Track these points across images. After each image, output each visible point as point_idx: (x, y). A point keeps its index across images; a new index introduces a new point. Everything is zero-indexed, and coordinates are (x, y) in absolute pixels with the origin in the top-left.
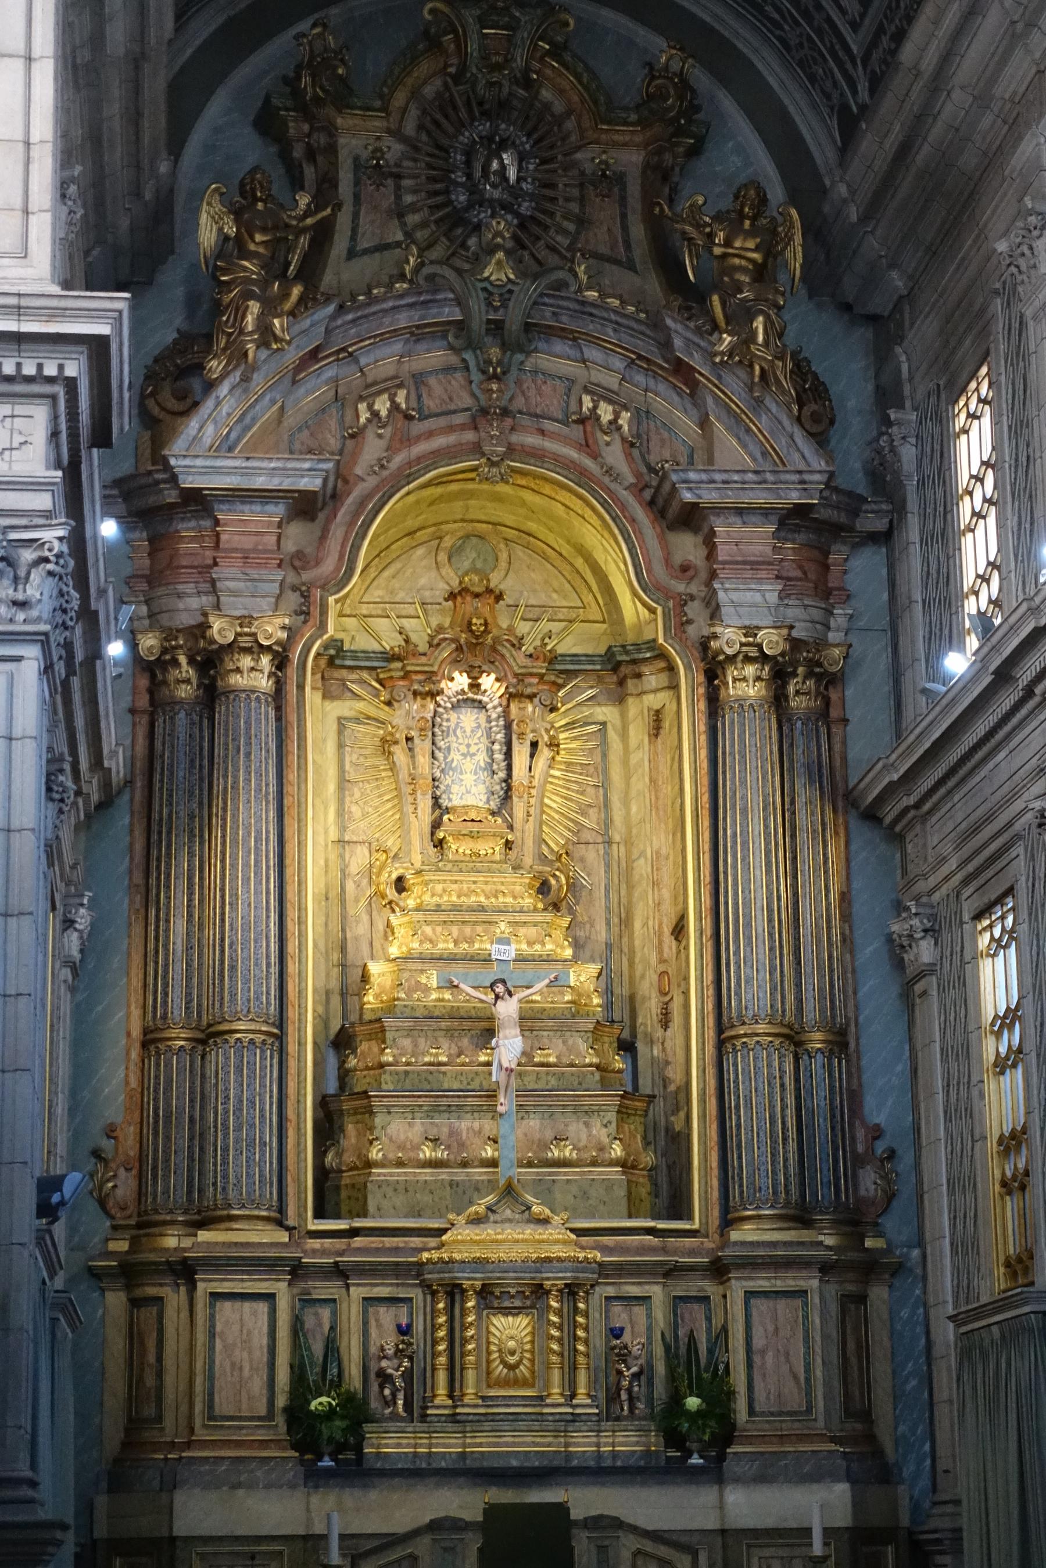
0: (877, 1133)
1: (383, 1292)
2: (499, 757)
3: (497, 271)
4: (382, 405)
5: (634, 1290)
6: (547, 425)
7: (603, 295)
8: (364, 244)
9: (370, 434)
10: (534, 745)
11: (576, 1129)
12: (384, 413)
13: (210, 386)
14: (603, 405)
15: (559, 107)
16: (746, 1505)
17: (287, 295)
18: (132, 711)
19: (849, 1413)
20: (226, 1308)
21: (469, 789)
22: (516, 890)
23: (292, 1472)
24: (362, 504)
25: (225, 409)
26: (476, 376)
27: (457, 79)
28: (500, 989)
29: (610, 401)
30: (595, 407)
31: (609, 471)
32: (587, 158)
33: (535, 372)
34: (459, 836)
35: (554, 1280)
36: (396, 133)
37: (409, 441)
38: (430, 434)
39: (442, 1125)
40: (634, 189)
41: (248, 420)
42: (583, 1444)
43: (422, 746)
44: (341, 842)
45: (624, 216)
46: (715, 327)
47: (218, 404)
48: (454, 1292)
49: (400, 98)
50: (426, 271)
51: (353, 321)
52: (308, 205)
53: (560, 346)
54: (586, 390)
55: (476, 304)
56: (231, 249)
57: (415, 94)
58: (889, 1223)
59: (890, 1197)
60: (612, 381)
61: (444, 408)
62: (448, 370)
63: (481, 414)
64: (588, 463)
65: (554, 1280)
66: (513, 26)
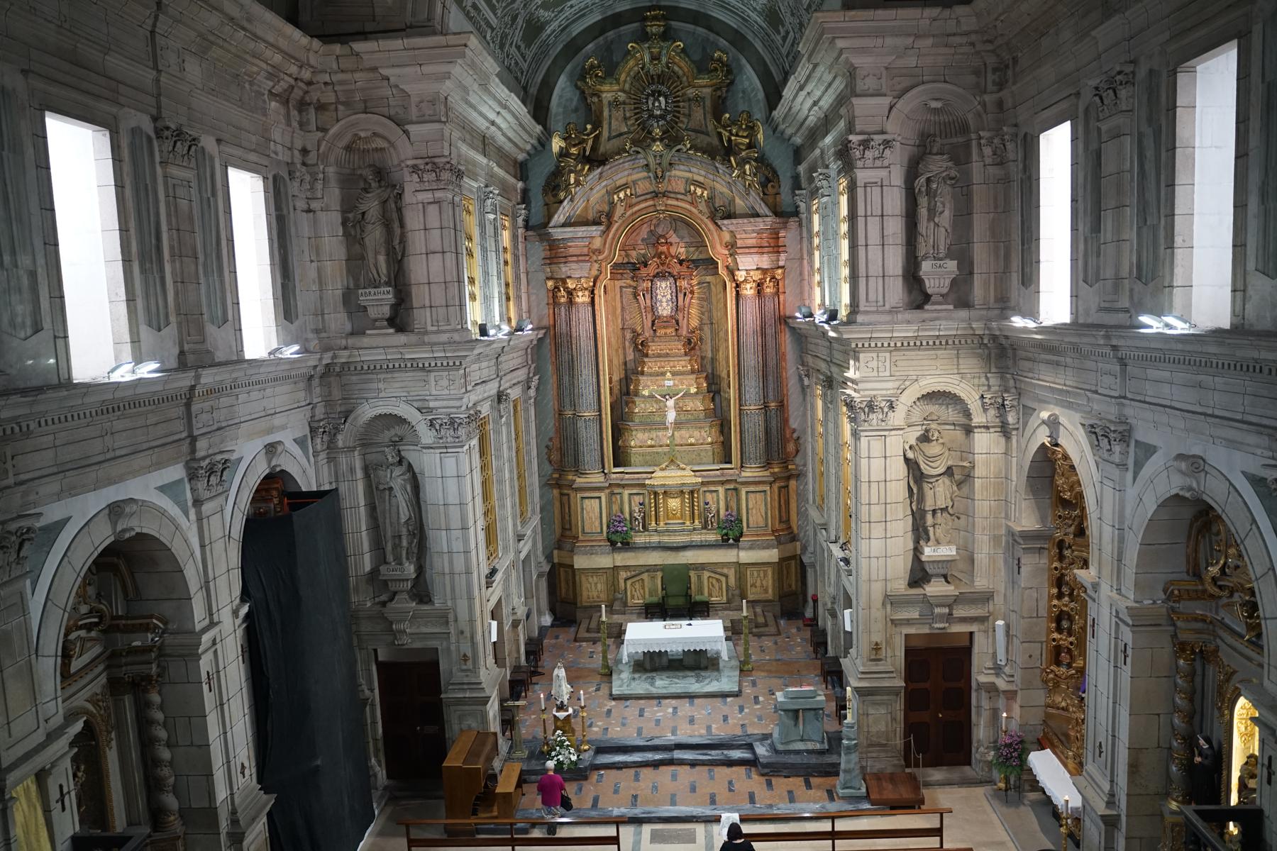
0: (794, 431)
1: (634, 491)
3: (658, 147)
4: (622, 195)
5: (713, 489)
11: (696, 433)
13: (561, 202)
15: (681, 73)
16: (745, 556)
19: (780, 522)
20: (586, 501)
21: (665, 309)
22: (678, 347)
23: (609, 548)
31: (701, 212)
32: (691, 92)
35: (686, 489)
36: (623, 91)
37: (631, 206)
38: (639, 203)
39: (654, 434)
40: (708, 103)
42: (697, 538)
43: (648, 296)
48: (656, 494)
49: (623, 76)
55: (651, 159)
56: (564, 154)
57: (628, 75)
58: (798, 460)
59: (797, 451)
60: (701, 179)
63: (656, 195)
65: (686, 489)
66: (661, 48)
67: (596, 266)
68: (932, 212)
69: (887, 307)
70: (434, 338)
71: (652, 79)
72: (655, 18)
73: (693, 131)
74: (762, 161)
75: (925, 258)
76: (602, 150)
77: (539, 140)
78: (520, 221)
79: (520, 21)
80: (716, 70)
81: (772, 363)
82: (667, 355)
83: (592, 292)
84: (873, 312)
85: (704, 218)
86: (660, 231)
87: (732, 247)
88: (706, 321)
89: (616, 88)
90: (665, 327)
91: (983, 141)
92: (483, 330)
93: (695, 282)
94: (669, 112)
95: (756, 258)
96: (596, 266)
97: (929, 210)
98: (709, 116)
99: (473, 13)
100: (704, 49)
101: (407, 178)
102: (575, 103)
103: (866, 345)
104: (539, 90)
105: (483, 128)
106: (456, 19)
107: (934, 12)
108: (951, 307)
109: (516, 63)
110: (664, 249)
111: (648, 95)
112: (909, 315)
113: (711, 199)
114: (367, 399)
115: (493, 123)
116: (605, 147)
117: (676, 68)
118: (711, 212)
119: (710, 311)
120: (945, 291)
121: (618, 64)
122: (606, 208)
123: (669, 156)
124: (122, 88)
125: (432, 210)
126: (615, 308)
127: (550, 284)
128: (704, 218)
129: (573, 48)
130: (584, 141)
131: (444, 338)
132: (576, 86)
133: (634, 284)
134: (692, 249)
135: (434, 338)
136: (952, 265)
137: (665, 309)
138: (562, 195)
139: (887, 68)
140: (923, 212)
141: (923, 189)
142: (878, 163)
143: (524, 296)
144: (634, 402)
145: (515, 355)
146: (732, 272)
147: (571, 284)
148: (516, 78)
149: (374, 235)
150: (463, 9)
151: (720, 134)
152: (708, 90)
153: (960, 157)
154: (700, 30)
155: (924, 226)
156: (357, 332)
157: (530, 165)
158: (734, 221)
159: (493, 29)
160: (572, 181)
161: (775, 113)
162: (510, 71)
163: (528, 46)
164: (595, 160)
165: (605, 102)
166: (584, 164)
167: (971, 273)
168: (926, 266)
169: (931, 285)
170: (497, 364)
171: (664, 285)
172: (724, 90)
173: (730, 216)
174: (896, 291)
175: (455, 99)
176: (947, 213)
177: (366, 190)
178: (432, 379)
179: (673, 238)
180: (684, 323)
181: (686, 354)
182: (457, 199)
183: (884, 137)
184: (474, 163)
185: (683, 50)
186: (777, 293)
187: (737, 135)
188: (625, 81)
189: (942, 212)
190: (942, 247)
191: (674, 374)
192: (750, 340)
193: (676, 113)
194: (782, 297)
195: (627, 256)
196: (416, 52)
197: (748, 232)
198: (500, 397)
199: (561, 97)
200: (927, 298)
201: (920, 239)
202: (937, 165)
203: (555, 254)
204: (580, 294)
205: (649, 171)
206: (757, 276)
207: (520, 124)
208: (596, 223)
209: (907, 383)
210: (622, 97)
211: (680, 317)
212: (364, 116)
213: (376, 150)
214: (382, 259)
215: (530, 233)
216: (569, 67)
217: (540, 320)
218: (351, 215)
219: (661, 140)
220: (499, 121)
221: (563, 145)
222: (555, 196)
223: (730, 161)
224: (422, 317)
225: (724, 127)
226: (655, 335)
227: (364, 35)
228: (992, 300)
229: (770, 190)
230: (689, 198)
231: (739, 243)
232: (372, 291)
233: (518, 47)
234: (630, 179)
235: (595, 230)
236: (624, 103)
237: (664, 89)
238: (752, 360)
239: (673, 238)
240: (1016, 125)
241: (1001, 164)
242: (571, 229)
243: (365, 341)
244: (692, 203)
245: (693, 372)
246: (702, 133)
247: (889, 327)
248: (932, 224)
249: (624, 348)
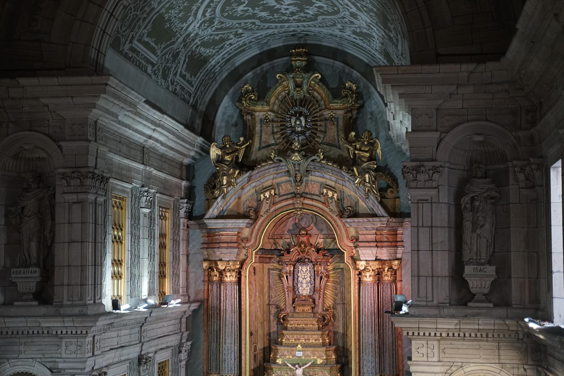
2: (313, 280)
3: (296, 157)
4: (267, 194)
6: (314, 197)
8: (263, 145)
9: (264, 203)
10: (321, 278)
12: (268, 197)
14: (329, 192)
15: (319, 97)
17: (235, 173)
18: (203, 281)
21: (305, 289)
22: (313, 323)
24: (262, 223)
25: (220, 204)
26: (294, 185)
27: (288, 94)
28: (297, 366)
29: (331, 190)
30: (327, 192)
33: (311, 181)
34: (299, 305)
36: (271, 111)
37: (274, 204)
38: (281, 201)
40: (341, 123)
41: (228, 204)
44: (269, 305)
45: (338, 131)
46: (355, 175)
47: (218, 204)
49: (273, 100)
50: (276, 158)
51: (258, 173)
52: (243, 141)
53: (317, 174)
54: (325, 188)
55: (291, 167)
56: (220, 160)
57: (277, 98)
60: (332, 184)
61: (286, 193)
62: (287, 181)
63: (295, 195)
64: (325, 209)
67: (244, 251)
68: (475, 225)
69: (435, 302)
70: (68, 311)
71: (295, 103)
72: (299, 54)
73: (328, 144)
74: (382, 170)
75: (469, 263)
76: (253, 157)
77: (202, 149)
78: (182, 212)
79: (182, 57)
80: (346, 96)
81: (388, 340)
82: (303, 329)
83: (240, 273)
84: (423, 306)
85: (334, 216)
86: (303, 224)
87: (355, 240)
88: (339, 301)
89: (267, 108)
90: (303, 305)
91: (516, 169)
92: (116, 305)
93: (330, 268)
94: (308, 129)
95: (374, 250)
96: (244, 251)
97: (473, 223)
98: (342, 135)
99: (130, 54)
100: (341, 79)
101: (58, 182)
102: (235, 119)
103: (416, 334)
104: (207, 108)
105: (142, 141)
106: (111, 60)
107: (471, 67)
108: (491, 305)
109: (183, 88)
110: (305, 239)
111: (292, 115)
112: (452, 311)
113: (340, 200)
114: (8, 359)
115: (150, 137)
116: (256, 154)
117: (316, 94)
118: (341, 211)
119: (343, 293)
120: (486, 291)
121: (270, 88)
122: (255, 204)
123: (305, 164)
125: (76, 208)
126: (262, 287)
127: (205, 265)
128: (334, 216)
129: (236, 75)
130: (237, 150)
131: (76, 310)
132: (235, 105)
133: (280, 267)
134: (329, 240)
135: (68, 311)
136: (491, 270)
137: (305, 289)
138: (217, 192)
139: (437, 109)
140: (467, 225)
141: (468, 206)
142: (428, 184)
143: (182, 275)
144: (272, 369)
145: (166, 324)
146: (354, 260)
147: (221, 266)
148: (184, 99)
149: (30, 225)
150: (121, 52)
151: (348, 149)
152: (341, 112)
153: (499, 181)
154: (338, 64)
155: (467, 236)
156: (8, 303)
157: (196, 167)
158: (356, 220)
159: (153, 65)
160: (225, 182)
161: (390, 133)
162: (177, 95)
163: (194, 74)
164: (246, 165)
165: (258, 119)
166: (235, 169)
167: (510, 277)
168: (468, 270)
170: (141, 332)
171: (304, 269)
172: (355, 112)
173: (355, 215)
175: (105, 121)
176: (487, 226)
177: (27, 190)
178: (64, 344)
179: (314, 231)
180: (319, 302)
181: (319, 329)
182: (101, 199)
183: (436, 164)
184: (129, 169)
185: (320, 80)
186: (394, 281)
187: (360, 150)
188: (274, 103)
189: (482, 226)
190: (483, 255)
191: (304, 346)
192: (369, 321)
193: (314, 130)
194: (399, 285)
195: (275, 243)
196: (68, 88)
197: (367, 228)
198: (141, 360)
199: (224, 114)
200: (471, 297)
201: (465, 247)
202: (480, 187)
203: (211, 240)
204: (228, 274)
205: (290, 176)
206: (375, 266)
207: (178, 137)
208: (244, 216)
209: (454, 369)
210: (271, 115)
211: (316, 296)
212: (28, 133)
213: (39, 159)
214: (34, 245)
215: (192, 222)
216: (231, 91)
217: (196, 294)
218: (13, 209)
219: (299, 152)
220: (155, 135)
221: (219, 153)
222: (213, 193)
223: (353, 171)
224: (62, 294)
225: (350, 143)
226: (295, 312)
227: (32, 72)
228: (527, 300)
229: (389, 194)
230: (322, 199)
231: (361, 238)
232: (22, 270)
233: (184, 77)
234: (275, 181)
235: (242, 223)
236: (273, 121)
237: (305, 110)
238: (369, 337)
239: (314, 231)
240: (542, 157)
241: (533, 187)
242: (223, 221)
243: (12, 311)
244: (324, 203)
245: (324, 345)
246: (335, 146)
247: (433, 320)
248: (475, 235)
249: (269, 321)
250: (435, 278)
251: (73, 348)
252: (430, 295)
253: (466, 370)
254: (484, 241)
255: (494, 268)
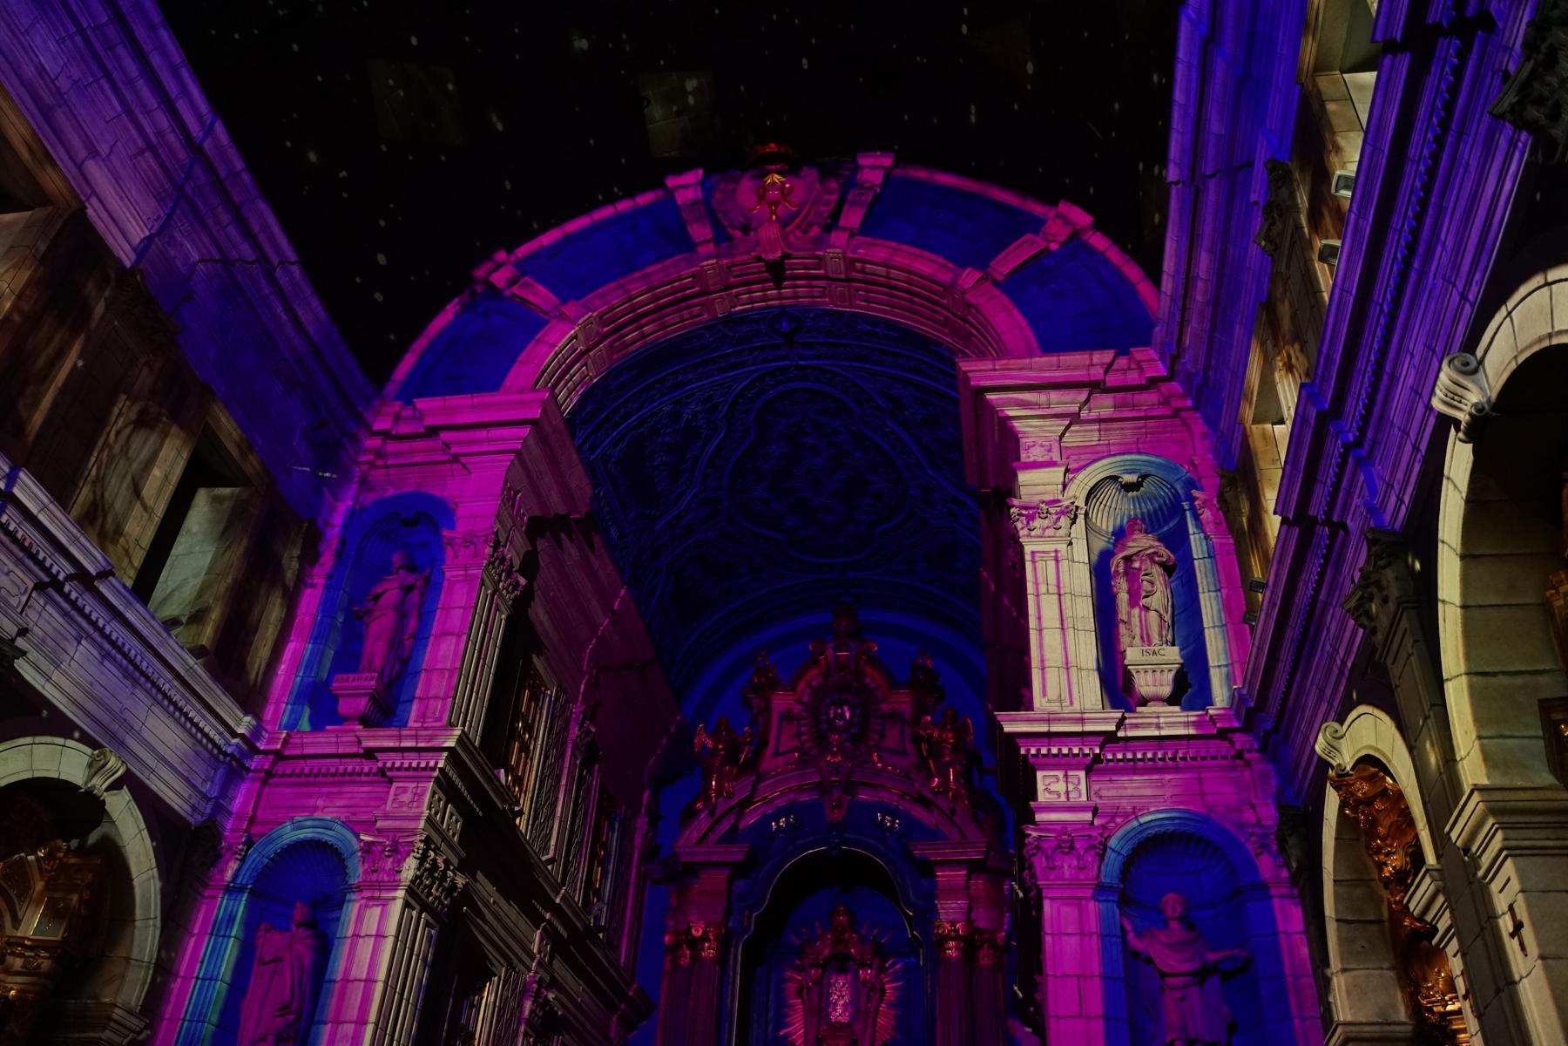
7: (885, 766)
32: (885, 707)
36: (799, 702)
49: (802, 686)
120: (1166, 690)
124: (94, 200)
141: (1121, 570)
169: (1144, 684)
174: (1090, 692)
201: (1122, 629)
210: (798, 708)
250: (1073, 671)
251: (406, 798)
252: (1065, 695)
253: (1143, 820)
254: (1153, 616)
255: (1176, 649)
